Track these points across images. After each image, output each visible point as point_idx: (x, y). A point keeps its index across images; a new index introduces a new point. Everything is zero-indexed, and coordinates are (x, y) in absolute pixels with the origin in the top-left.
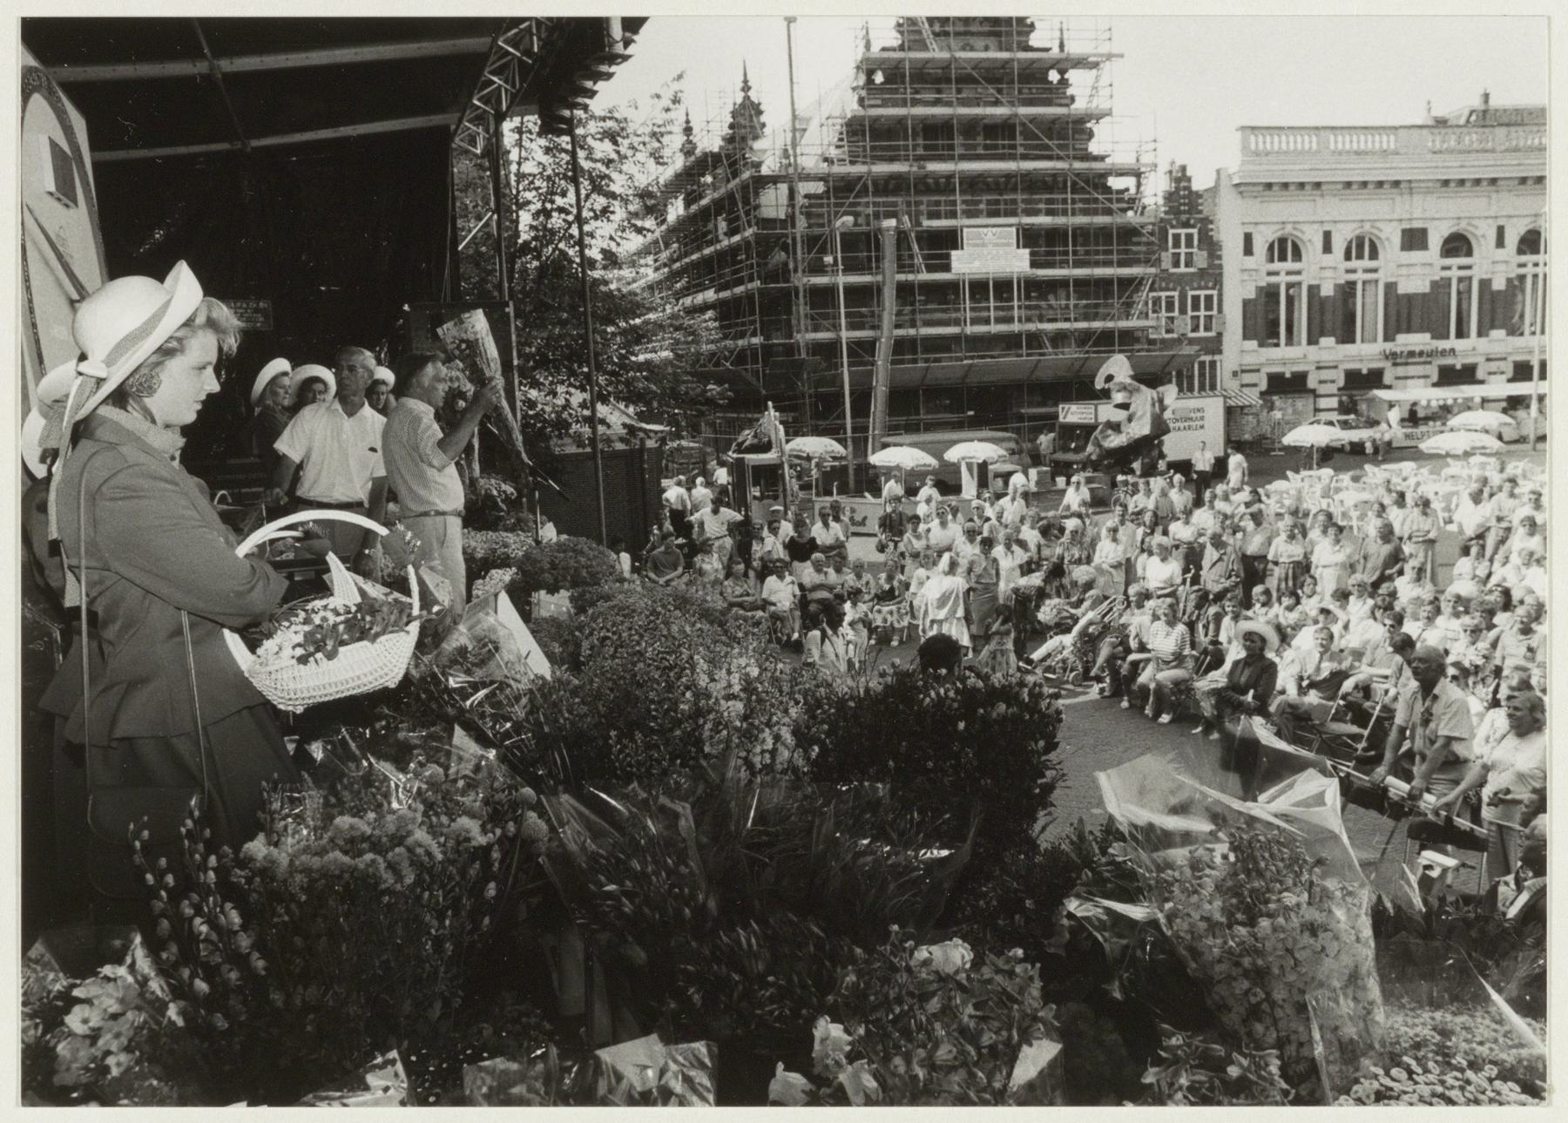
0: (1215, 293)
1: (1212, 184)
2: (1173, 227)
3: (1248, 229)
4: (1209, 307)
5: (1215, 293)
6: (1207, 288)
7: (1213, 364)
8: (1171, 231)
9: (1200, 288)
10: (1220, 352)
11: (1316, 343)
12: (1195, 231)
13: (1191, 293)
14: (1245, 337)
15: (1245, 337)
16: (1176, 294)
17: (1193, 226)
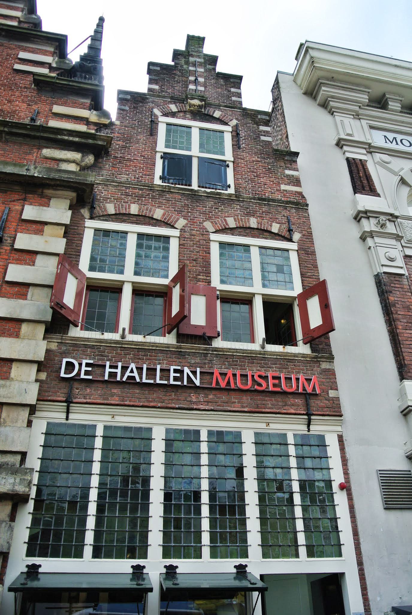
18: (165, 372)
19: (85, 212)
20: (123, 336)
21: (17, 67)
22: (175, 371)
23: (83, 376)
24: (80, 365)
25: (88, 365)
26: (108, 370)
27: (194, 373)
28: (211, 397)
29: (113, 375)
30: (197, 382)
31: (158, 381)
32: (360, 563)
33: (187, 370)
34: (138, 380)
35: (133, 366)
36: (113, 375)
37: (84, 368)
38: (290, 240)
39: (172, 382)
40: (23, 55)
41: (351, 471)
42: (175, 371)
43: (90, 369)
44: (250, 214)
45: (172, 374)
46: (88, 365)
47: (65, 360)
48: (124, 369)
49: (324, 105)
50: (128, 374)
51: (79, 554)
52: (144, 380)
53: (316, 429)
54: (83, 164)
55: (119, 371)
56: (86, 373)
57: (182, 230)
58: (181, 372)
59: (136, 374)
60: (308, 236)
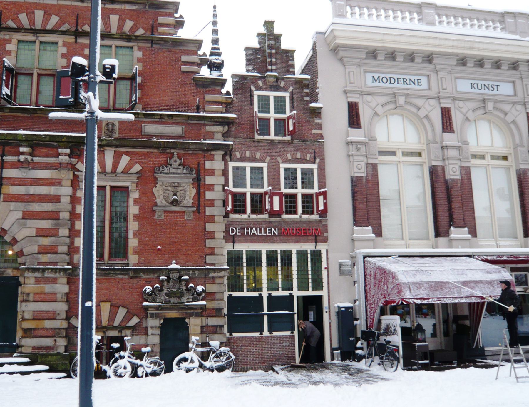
0: (315, 167)
1: (311, 53)
2: (258, 88)
3: (353, 99)
4: (307, 183)
5: (315, 167)
6: (303, 160)
7: (316, 255)
8: (256, 93)
9: (296, 160)
10: (325, 240)
11: (447, 234)
12: (287, 95)
13: (283, 166)
14: (357, 222)
15: (357, 222)
16: (264, 165)
17: (285, 90)
18: (265, 229)
19: (228, 158)
20: (249, 217)
21: (184, 68)
22: (269, 230)
23: (237, 234)
24: (236, 229)
25: (239, 229)
26: (246, 231)
27: (275, 230)
28: (281, 238)
29: (247, 233)
30: (277, 234)
31: (263, 234)
32: (329, 292)
33: (273, 229)
34: (256, 234)
35: (254, 229)
36: (247, 233)
37: (238, 231)
38: (314, 163)
39: (268, 234)
40: (184, 58)
41: (329, 263)
42: (269, 230)
43: (239, 231)
44: (297, 151)
45: (268, 231)
46: (239, 229)
47: (231, 228)
48: (251, 229)
49: (341, 60)
50: (253, 232)
51: (243, 291)
52: (258, 234)
53: (318, 248)
54: (224, 132)
55: (249, 231)
56: (239, 233)
57: (268, 164)
58: (271, 230)
59: (255, 232)
60: (323, 160)
